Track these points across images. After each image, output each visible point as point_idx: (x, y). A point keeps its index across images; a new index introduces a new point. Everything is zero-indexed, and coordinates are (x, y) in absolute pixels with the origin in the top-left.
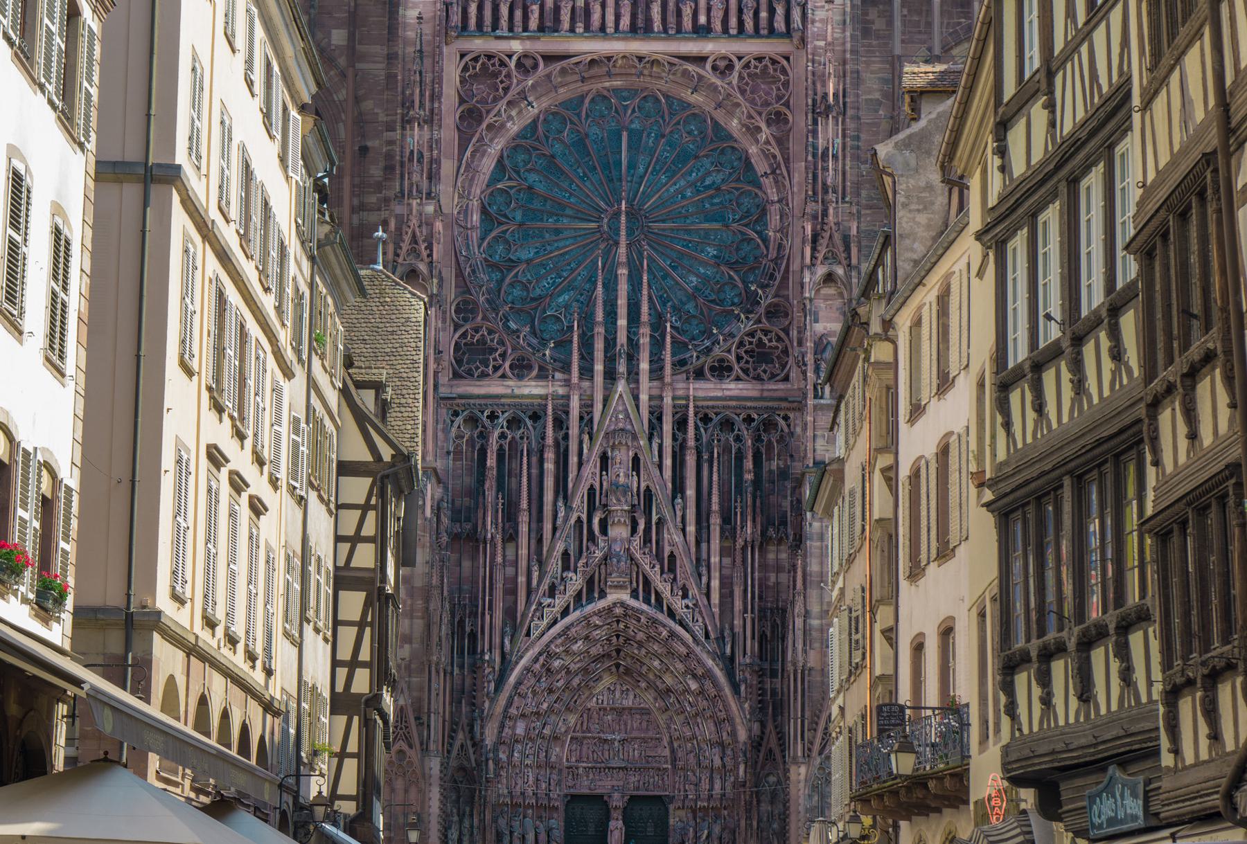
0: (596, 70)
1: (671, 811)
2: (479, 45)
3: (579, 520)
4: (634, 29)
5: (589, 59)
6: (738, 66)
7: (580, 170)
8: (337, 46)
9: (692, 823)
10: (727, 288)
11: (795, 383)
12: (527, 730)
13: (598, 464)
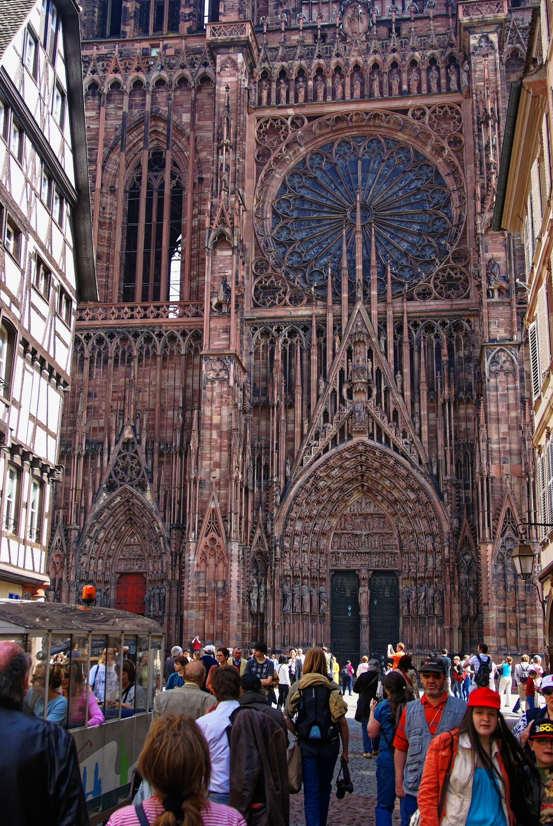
0: (341, 125)
1: (400, 580)
2: (268, 113)
3: (334, 391)
4: (362, 95)
5: (335, 116)
6: (428, 112)
7: (332, 185)
8: (186, 123)
9: (414, 588)
10: (427, 249)
11: (473, 300)
12: (304, 527)
13: (346, 355)
